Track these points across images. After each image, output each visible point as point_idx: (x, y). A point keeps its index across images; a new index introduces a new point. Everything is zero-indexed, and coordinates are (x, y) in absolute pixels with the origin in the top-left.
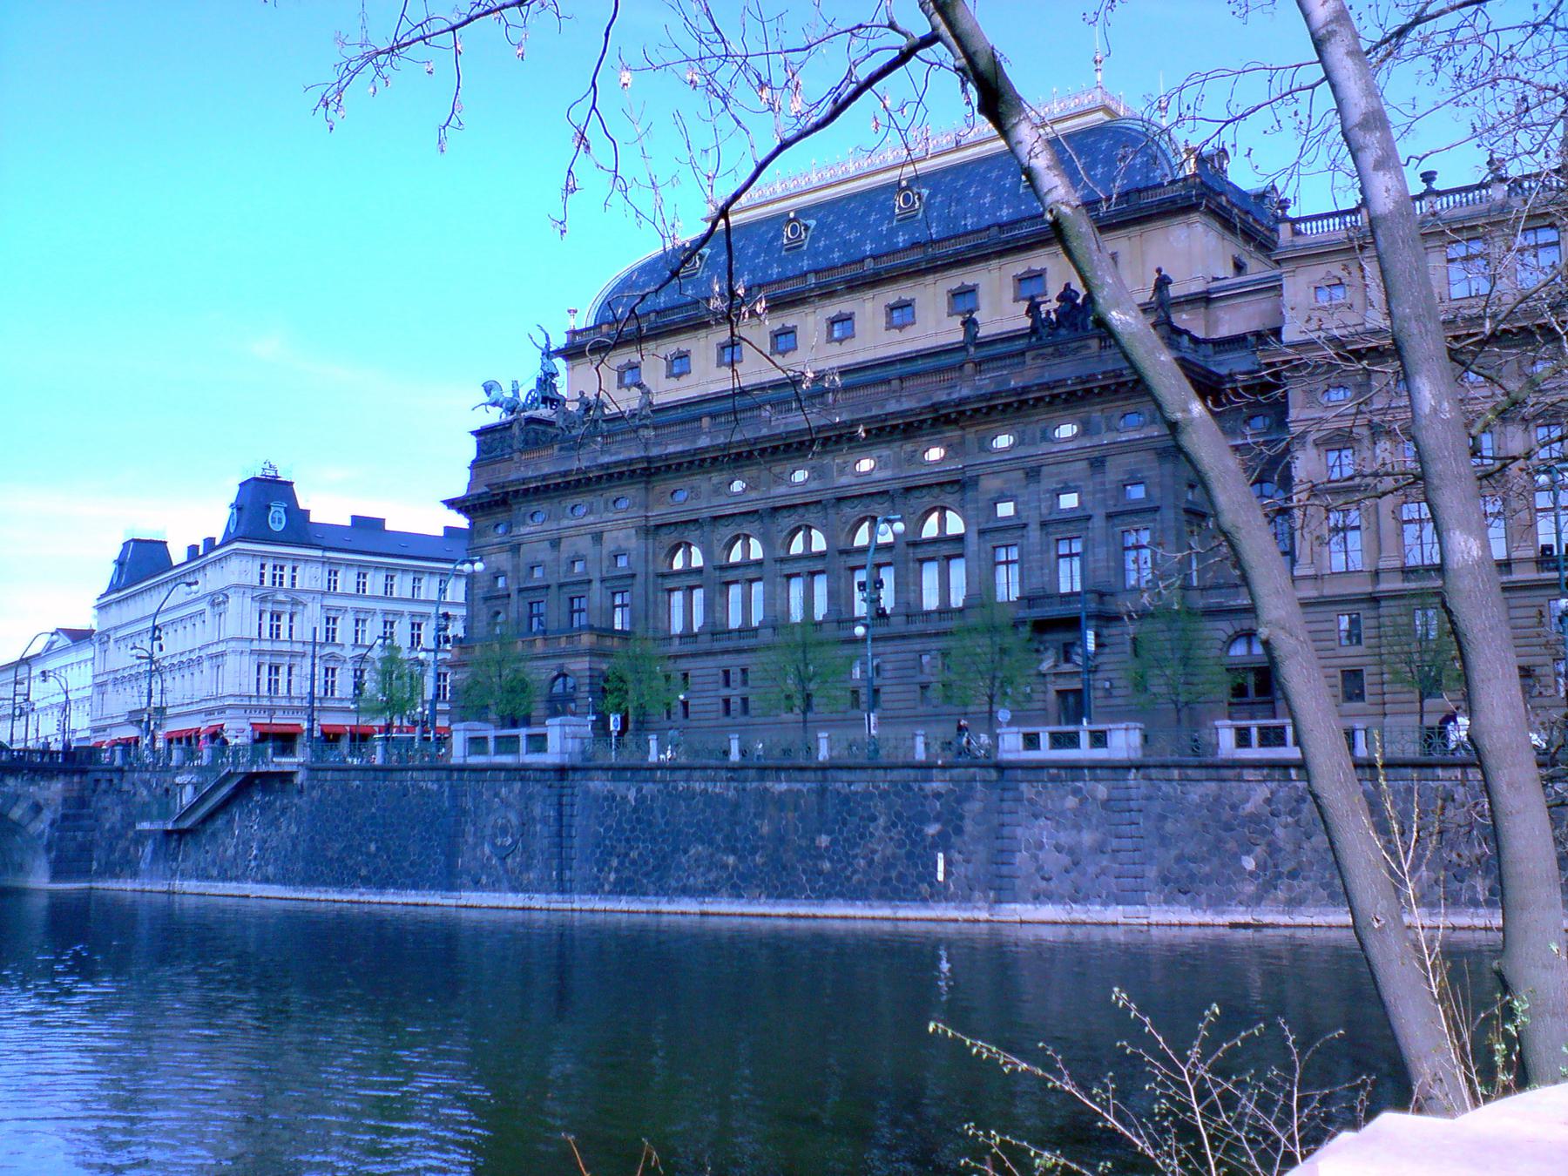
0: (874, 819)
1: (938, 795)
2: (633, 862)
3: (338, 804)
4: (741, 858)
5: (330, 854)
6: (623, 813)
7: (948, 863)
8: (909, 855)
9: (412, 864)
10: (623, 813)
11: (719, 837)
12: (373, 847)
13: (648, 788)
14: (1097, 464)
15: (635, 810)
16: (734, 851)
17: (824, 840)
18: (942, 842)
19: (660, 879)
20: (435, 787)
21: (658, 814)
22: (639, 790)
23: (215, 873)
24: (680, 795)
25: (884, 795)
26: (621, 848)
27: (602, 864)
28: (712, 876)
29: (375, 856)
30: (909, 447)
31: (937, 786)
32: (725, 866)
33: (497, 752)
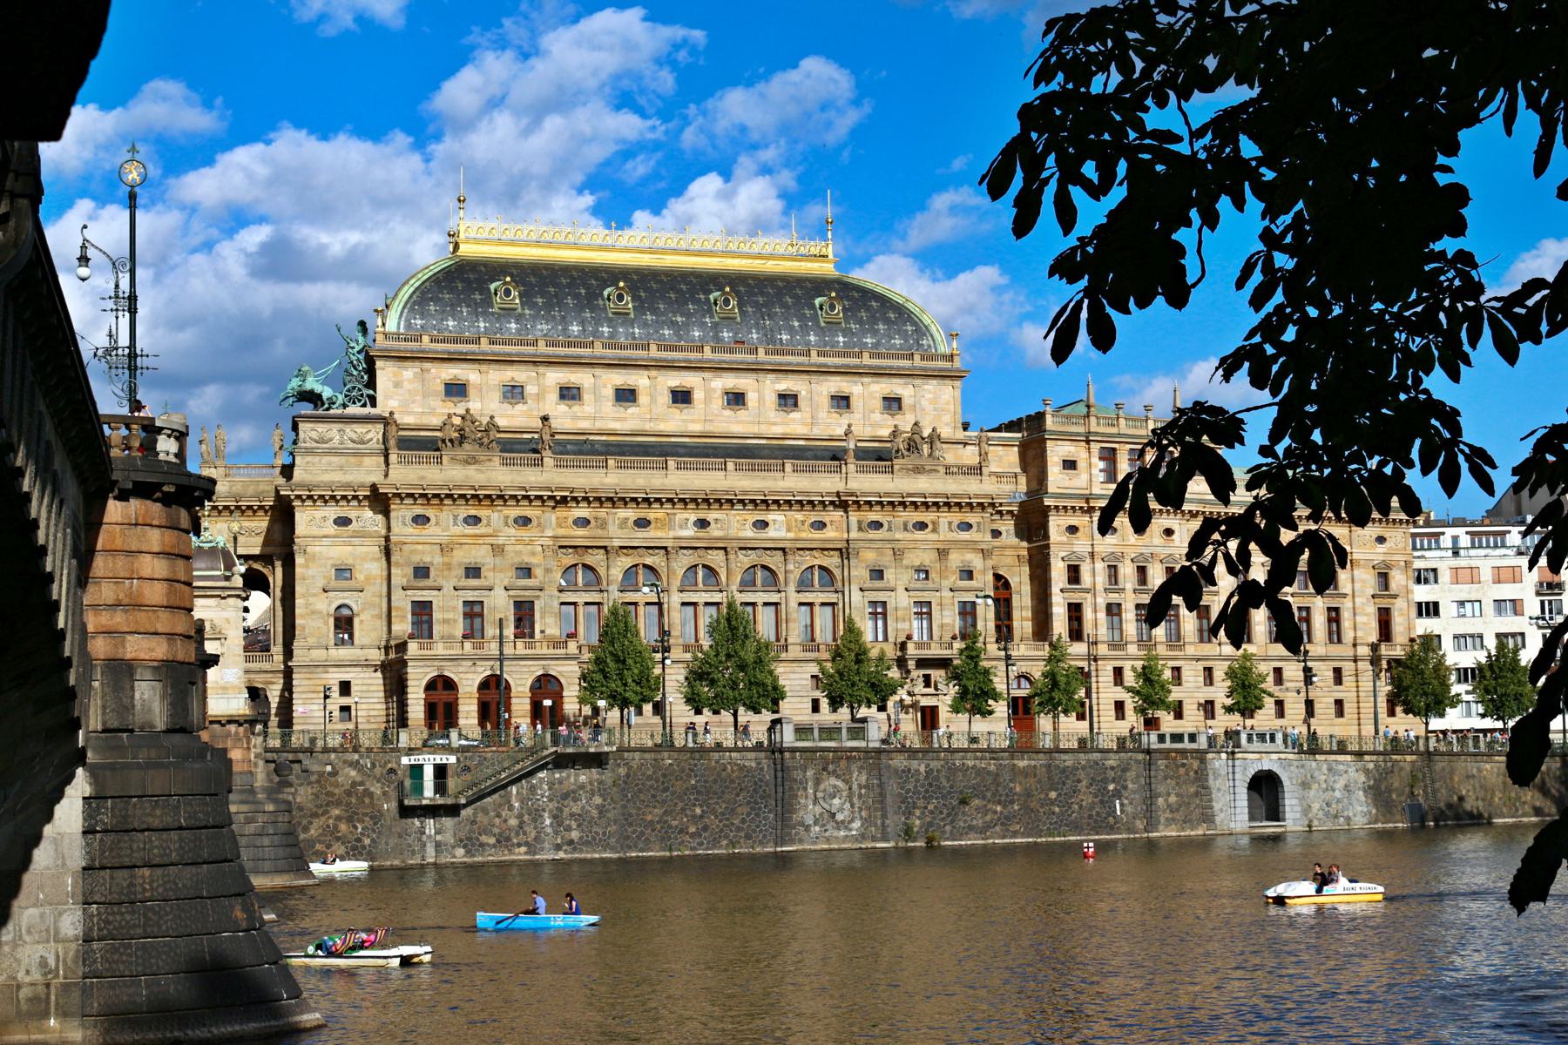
0: (1079, 781)
1: (1112, 768)
2: (932, 812)
3: (649, 778)
4: (1004, 807)
5: (649, 818)
6: (917, 781)
7: (1122, 805)
8: (1102, 802)
9: (743, 821)
10: (917, 781)
11: (989, 795)
12: (698, 811)
13: (934, 764)
14: (942, 553)
15: (927, 778)
16: (999, 803)
17: (1053, 795)
18: (1117, 794)
19: (952, 821)
20: (753, 764)
21: (945, 783)
22: (927, 766)
23: (492, 841)
24: (958, 769)
25: (1084, 768)
26: (921, 803)
27: (909, 814)
28: (988, 818)
29: (701, 817)
30: (799, 516)
31: (1111, 763)
32: (995, 812)
33: (821, 740)
